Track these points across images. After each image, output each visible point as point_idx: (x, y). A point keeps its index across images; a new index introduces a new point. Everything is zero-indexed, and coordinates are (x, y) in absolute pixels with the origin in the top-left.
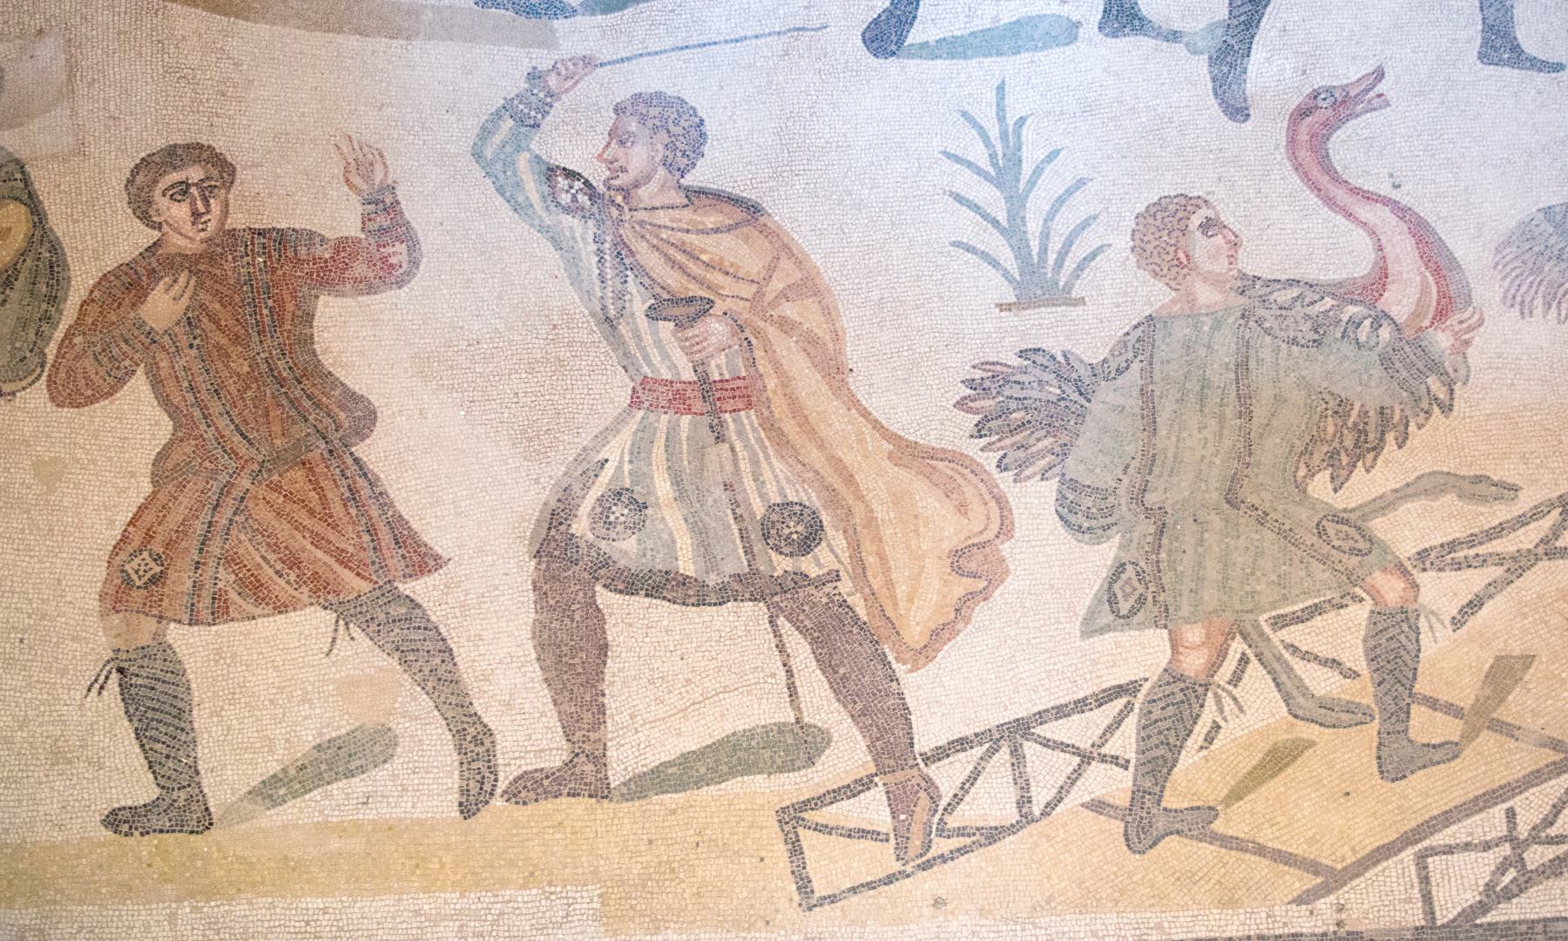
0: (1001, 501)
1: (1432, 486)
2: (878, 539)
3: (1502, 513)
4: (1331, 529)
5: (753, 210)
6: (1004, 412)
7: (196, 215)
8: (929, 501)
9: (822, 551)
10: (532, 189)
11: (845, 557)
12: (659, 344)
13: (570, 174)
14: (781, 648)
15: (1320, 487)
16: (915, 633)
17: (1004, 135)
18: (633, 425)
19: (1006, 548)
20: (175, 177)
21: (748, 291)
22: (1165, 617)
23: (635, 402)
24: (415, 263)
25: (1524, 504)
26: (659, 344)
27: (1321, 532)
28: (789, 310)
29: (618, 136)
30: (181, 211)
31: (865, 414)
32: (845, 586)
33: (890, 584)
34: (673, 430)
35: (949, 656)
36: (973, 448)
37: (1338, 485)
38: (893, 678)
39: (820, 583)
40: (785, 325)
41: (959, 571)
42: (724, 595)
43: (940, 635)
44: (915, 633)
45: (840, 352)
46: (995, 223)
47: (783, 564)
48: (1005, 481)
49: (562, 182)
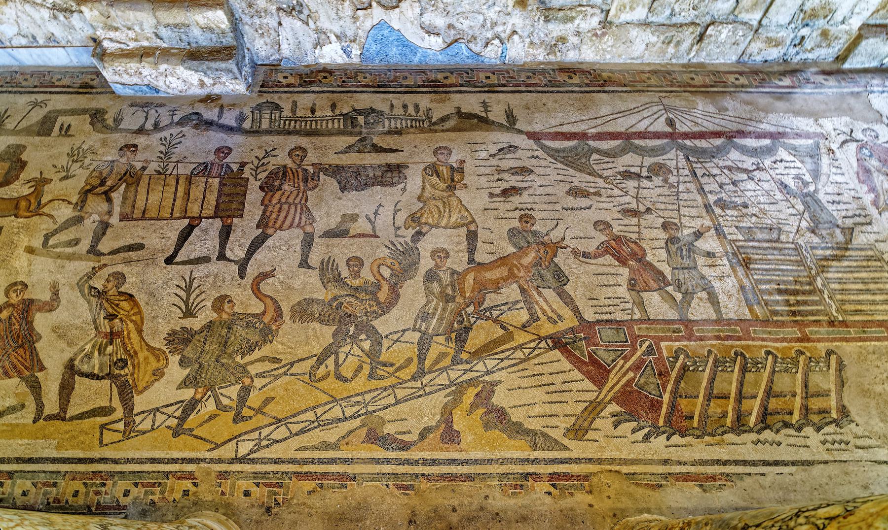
0: (167, 359)
1: (261, 360)
2: (139, 367)
3: (277, 365)
4: (238, 367)
5: (131, 296)
6: (174, 340)
7: (17, 295)
8: (152, 359)
9: (126, 370)
10: (87, 291)
11: (131, 371)
12: (104, 324)
13: (95, 288)
14: (111, 390)
15: (238, 359)
16: (140, 388)
17: (190, 282)
18: (94, 341)
19: (165, 370)
20: (16, 288)
21: (126, 313)
22: (196, 386)
23: (95, 337)
24: (58, 306)
25: (283, 363)
26: (104, 324)
27: (235, 368)
28: (133, 318)
29: (108, 281)
30: (15, 295)
31: (144, 340)
32: (129, 377)
33: (138, 376)
34: (102, 342)
35: (146, 393)
36: (164, 348)
37: (242, 358)
38: (133, 397)
39: (124, 376)
40: (132, 321)
41: (154, 374)
42: (103, 378)
43: (146, 388)
44: (140, 388)
45: (142, 327)
46: (183, 300)
47: (117, 372)
48: (169, 355)
49: (93, 290)
